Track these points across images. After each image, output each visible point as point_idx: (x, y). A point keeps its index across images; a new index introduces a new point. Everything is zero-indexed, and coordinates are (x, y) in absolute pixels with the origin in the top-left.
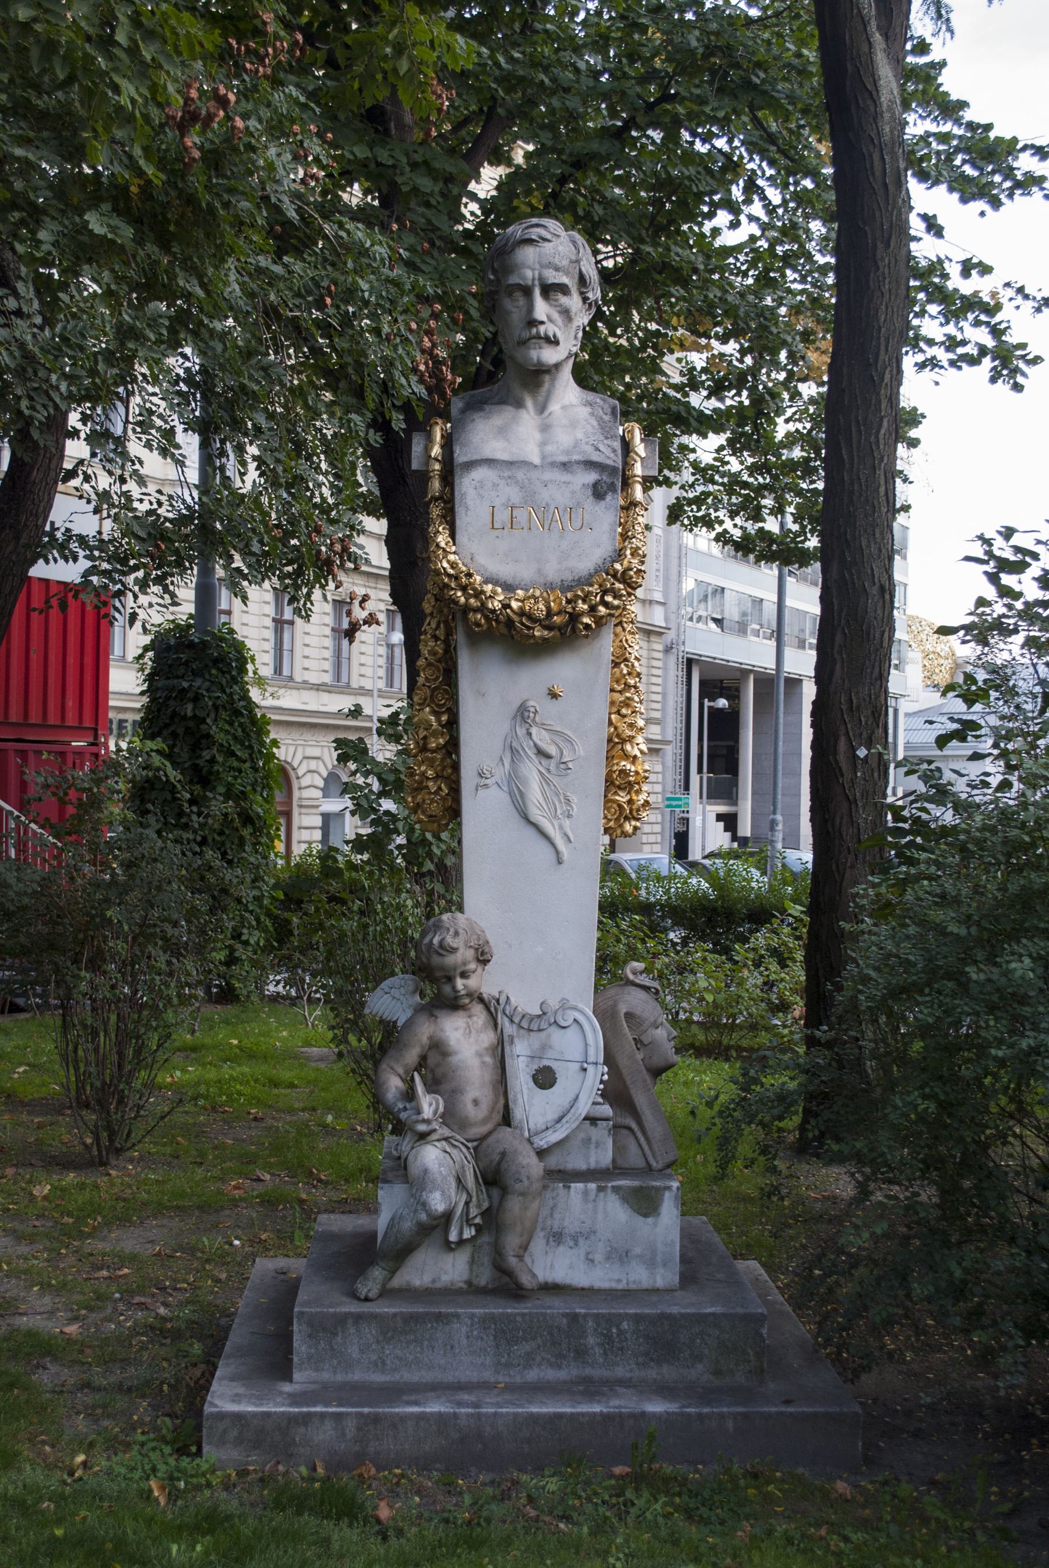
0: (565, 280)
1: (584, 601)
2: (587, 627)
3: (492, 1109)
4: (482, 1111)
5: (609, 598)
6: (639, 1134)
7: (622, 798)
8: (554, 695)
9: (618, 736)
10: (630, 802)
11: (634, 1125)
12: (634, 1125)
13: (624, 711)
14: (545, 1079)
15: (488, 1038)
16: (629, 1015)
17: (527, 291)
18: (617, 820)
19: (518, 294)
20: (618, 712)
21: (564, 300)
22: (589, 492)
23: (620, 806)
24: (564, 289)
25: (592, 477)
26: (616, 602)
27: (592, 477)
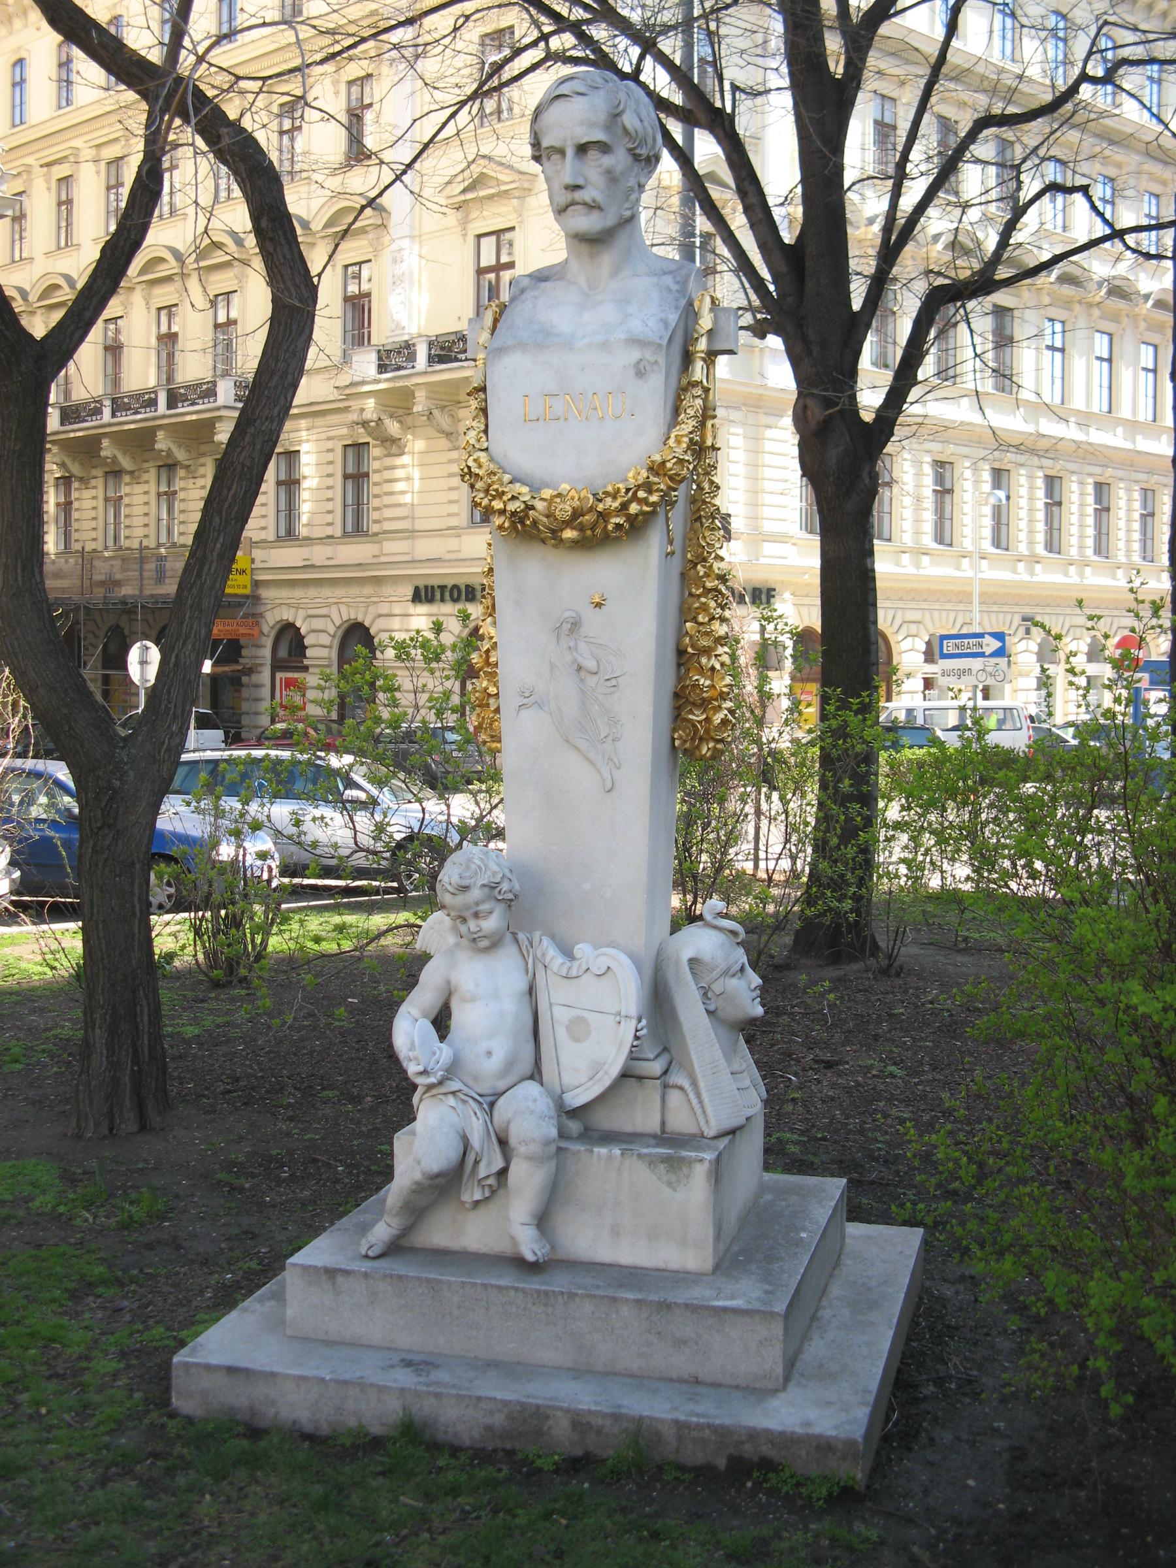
0: (600, 136)
1: (615, 498)
2: (618, 526)
3: (510, 1064)
4: (494, 1064)
5: (641, 494)
6: (692, 1095)
7: (698, 716)
8: (598, 605)
9: (693, 646)
10: (708, 720)
11: (686, 1084)
12: (686, 1084)
13: (701, 619)
14: (579, 1029)
15: (520, 983)
16: (692, 961)
17: (562, 152)
18: (693, 739)
19: (556, 157)
20: (694, 620)
21: (607, 161)
22: (632, 371)
23: (694, 726)
24: (604, 148)
25: (635, 355)
26: (654, 498)
27: (635, 355)
